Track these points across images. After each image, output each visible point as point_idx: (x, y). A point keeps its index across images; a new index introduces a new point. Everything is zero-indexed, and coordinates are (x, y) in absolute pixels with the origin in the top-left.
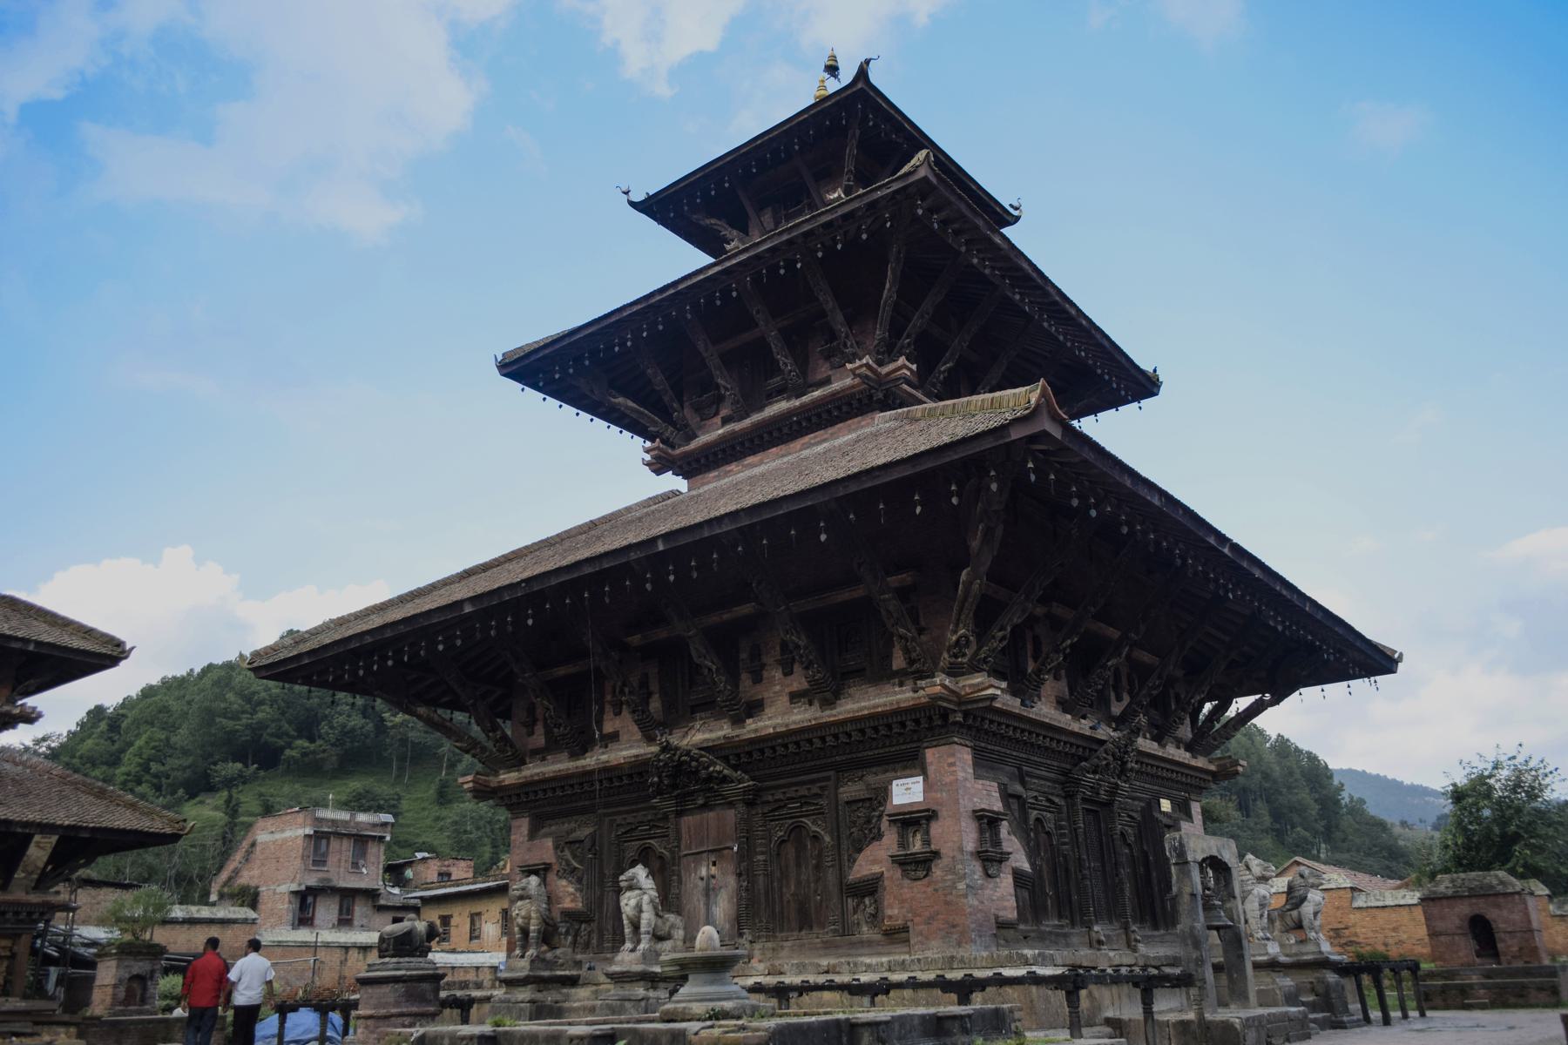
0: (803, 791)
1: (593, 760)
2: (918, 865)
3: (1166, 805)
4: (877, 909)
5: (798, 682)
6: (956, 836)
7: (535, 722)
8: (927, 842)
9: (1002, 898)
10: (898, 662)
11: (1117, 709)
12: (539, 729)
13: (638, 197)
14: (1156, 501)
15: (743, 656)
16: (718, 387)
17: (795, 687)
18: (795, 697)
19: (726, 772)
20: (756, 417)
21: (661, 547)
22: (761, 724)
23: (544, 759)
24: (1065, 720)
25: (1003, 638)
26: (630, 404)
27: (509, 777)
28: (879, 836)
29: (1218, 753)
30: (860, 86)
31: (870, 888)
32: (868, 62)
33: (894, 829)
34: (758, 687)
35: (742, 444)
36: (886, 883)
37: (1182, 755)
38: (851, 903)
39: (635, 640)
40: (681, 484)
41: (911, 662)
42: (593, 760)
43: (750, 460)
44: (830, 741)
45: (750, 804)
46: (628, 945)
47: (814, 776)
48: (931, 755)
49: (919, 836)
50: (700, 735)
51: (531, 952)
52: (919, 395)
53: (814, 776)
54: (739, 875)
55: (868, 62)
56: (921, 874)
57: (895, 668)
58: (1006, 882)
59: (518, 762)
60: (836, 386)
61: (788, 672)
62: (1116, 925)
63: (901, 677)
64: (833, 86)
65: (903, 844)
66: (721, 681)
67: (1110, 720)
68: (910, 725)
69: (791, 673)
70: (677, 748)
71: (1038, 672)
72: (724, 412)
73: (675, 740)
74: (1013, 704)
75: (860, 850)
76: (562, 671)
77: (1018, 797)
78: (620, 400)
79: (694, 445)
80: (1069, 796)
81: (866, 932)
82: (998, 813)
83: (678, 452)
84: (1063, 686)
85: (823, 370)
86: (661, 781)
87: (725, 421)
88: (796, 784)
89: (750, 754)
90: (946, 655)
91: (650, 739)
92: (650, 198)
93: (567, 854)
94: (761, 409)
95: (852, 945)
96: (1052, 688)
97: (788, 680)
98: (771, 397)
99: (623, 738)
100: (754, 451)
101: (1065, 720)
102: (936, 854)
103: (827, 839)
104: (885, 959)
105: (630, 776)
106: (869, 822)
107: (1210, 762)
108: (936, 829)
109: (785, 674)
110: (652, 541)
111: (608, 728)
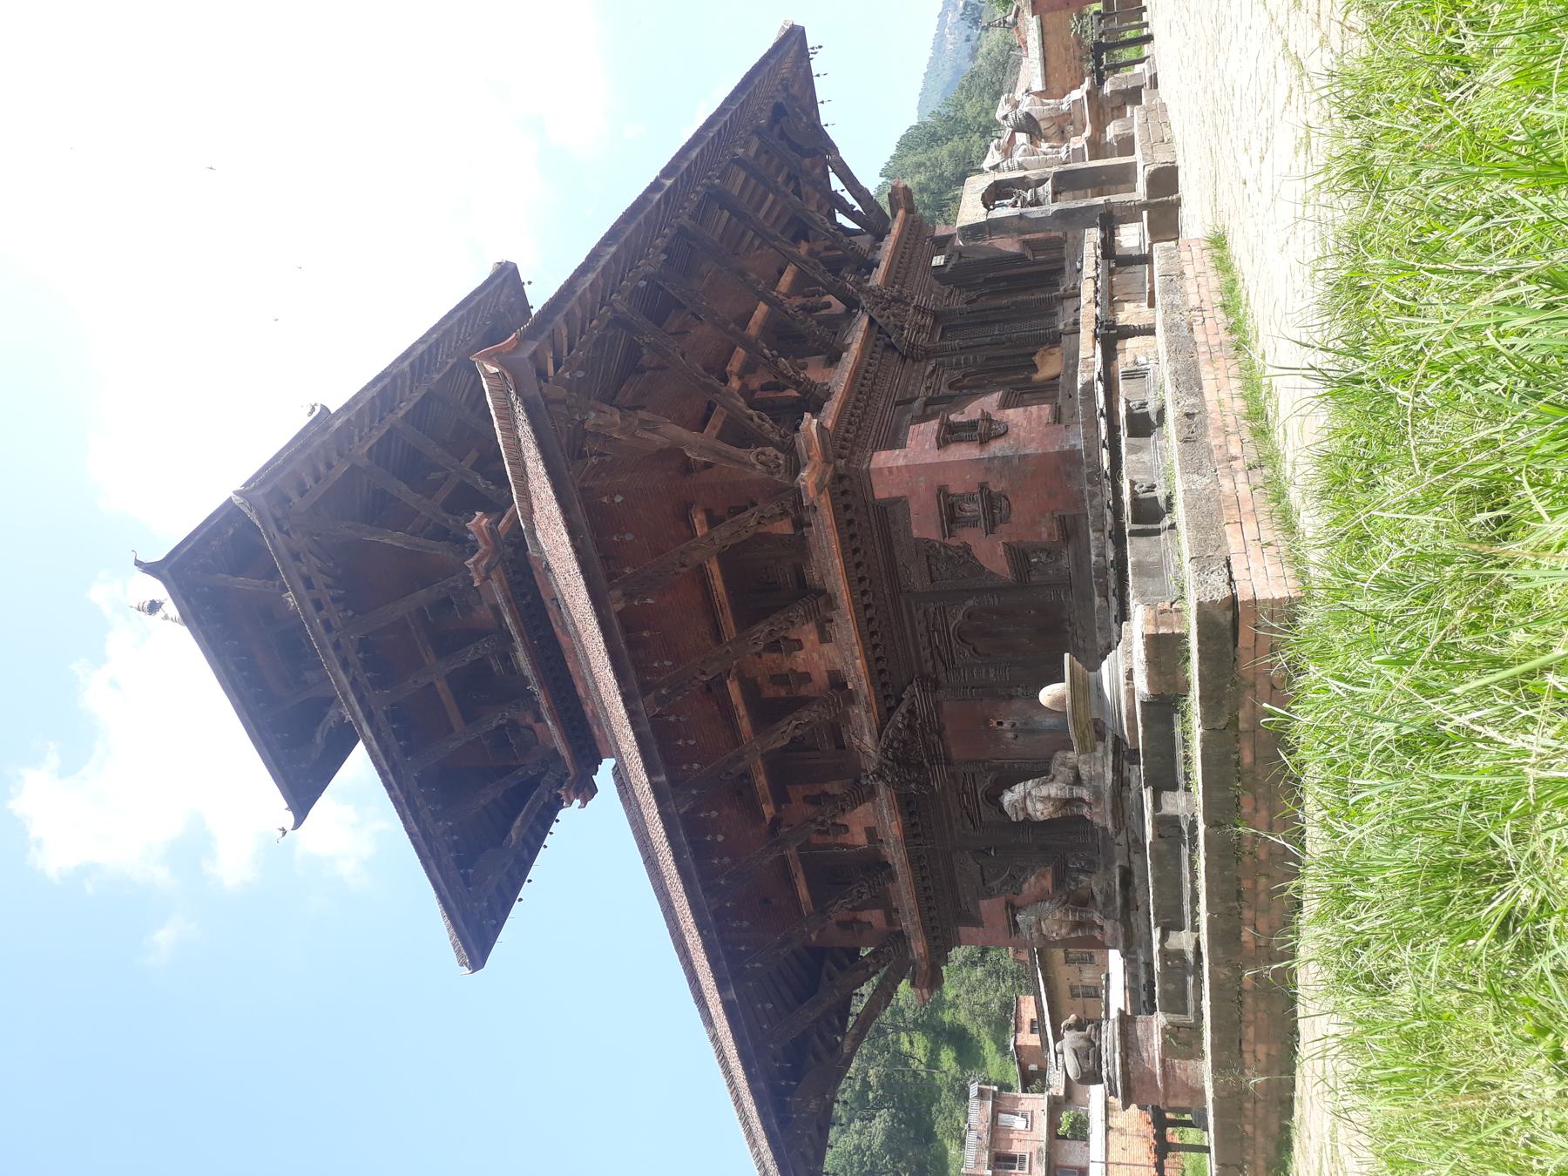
0: (923, 625)
1: (896, 855)
2: (994, 507)
3: (938, 261)
4: (1042, 550)
5: (808, 634)
7: (855, 921)
8: (971, 499)
9: (1029, 421)
10: (784, 527)
11: (838, 307)
12: (865, 916)
13: (289, 818)
14: (613, 249)
15: (783, 693)
16: (500, 728)
19: (903, 710)
20: (534, 687)
21: (663, 778)
23: (897, 910)
24: (850, 358)
25: (760, 417)
26: (518, 823)
27: (918, 947)
28: (967, 548)
29: (888, 211)
30: (165, 572)
31: (1018, 555)
32: (138, 563)
33: (958, 532)
34: (815, 676)
36: (1014, 540)
37: (889, 244)
38: (1035, 578)
39: (768, 810)
40: (607, 765)
41: (784, 513)
42: (896, 855)
43: (581, 691)
45: (937, 685)
46: (1085, 811)
47: (906, 617)
48: (881, 492)
49: (966, 506)
50: (866, 740)
51: (1097, 918)
52: (510, 511)
53: (906, 617)
54: (1011, 697)
55: (138, 563)
56: (1004, 503)
57: (791, 531)
58: (1013, 415)
59: (901, 938)
60: (500, 599)
62: (1059, 309)
63: (799, 524)
64: (170, 608)
66: (806, 716)
67: (849, 315)
70: (880, 763)
71: (798, 384)
72: (529, 720)
73: (872, 767)
74: (831, 408)
75: (982, 567)
76: (803, 892)
77: (926, 404)
78: (513, 834)
79: (564, 751)
80: (928, 354)
81: (1066, 561)
82: (941, 424)
83: (571, 770)
84: (813, 361)
86: (915, 781)
87: (539, 718)
88: (915, 637)
89: (884, 685)
90: (777, 477)
91: (872, 793)
92: (291, 808)
93: (995, 884)
94: (526, 681)
96: (815, 373)
97: (807, 645)
98: (513, 671)
99: (872, 822)
101: (850, 358)
102: (983, 486)
103: (970, 603)
104: (1092, 536)
105: (911, 814)
106: (951, 558)
107: (894, 216)
108: (956, 488)
109: (801, 648)
111: (861, 839)
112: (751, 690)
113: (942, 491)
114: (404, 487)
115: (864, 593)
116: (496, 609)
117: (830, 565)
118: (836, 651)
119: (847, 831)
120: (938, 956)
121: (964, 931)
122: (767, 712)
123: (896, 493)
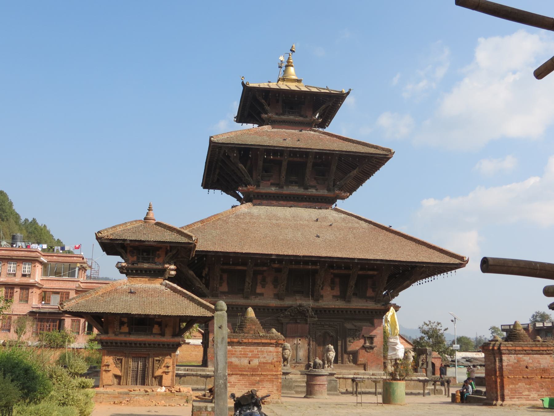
17: (335, 294)
18: (334, 297)
22: (324, 303)
32: (350, 90)
35: (282, 197)
38: (345, 356)
43: (282, 202)
44: (349, 312)
45: (313, 324)
48: (376, 321)
55: (350, 90)
57: (368, 295)
61: (332, 289)
63: (371, 298)
68: (374, 313)
72: (272, 181)
85: (313, 183)
87: (272, 184)
89: (320, 311)
95: (346, 366)
100: (284, 200)
105: (272, 310)
110: (354, 259)
115: (351, 311)
117: (358, 304)
119: (262, 287)
123: (376, 325)
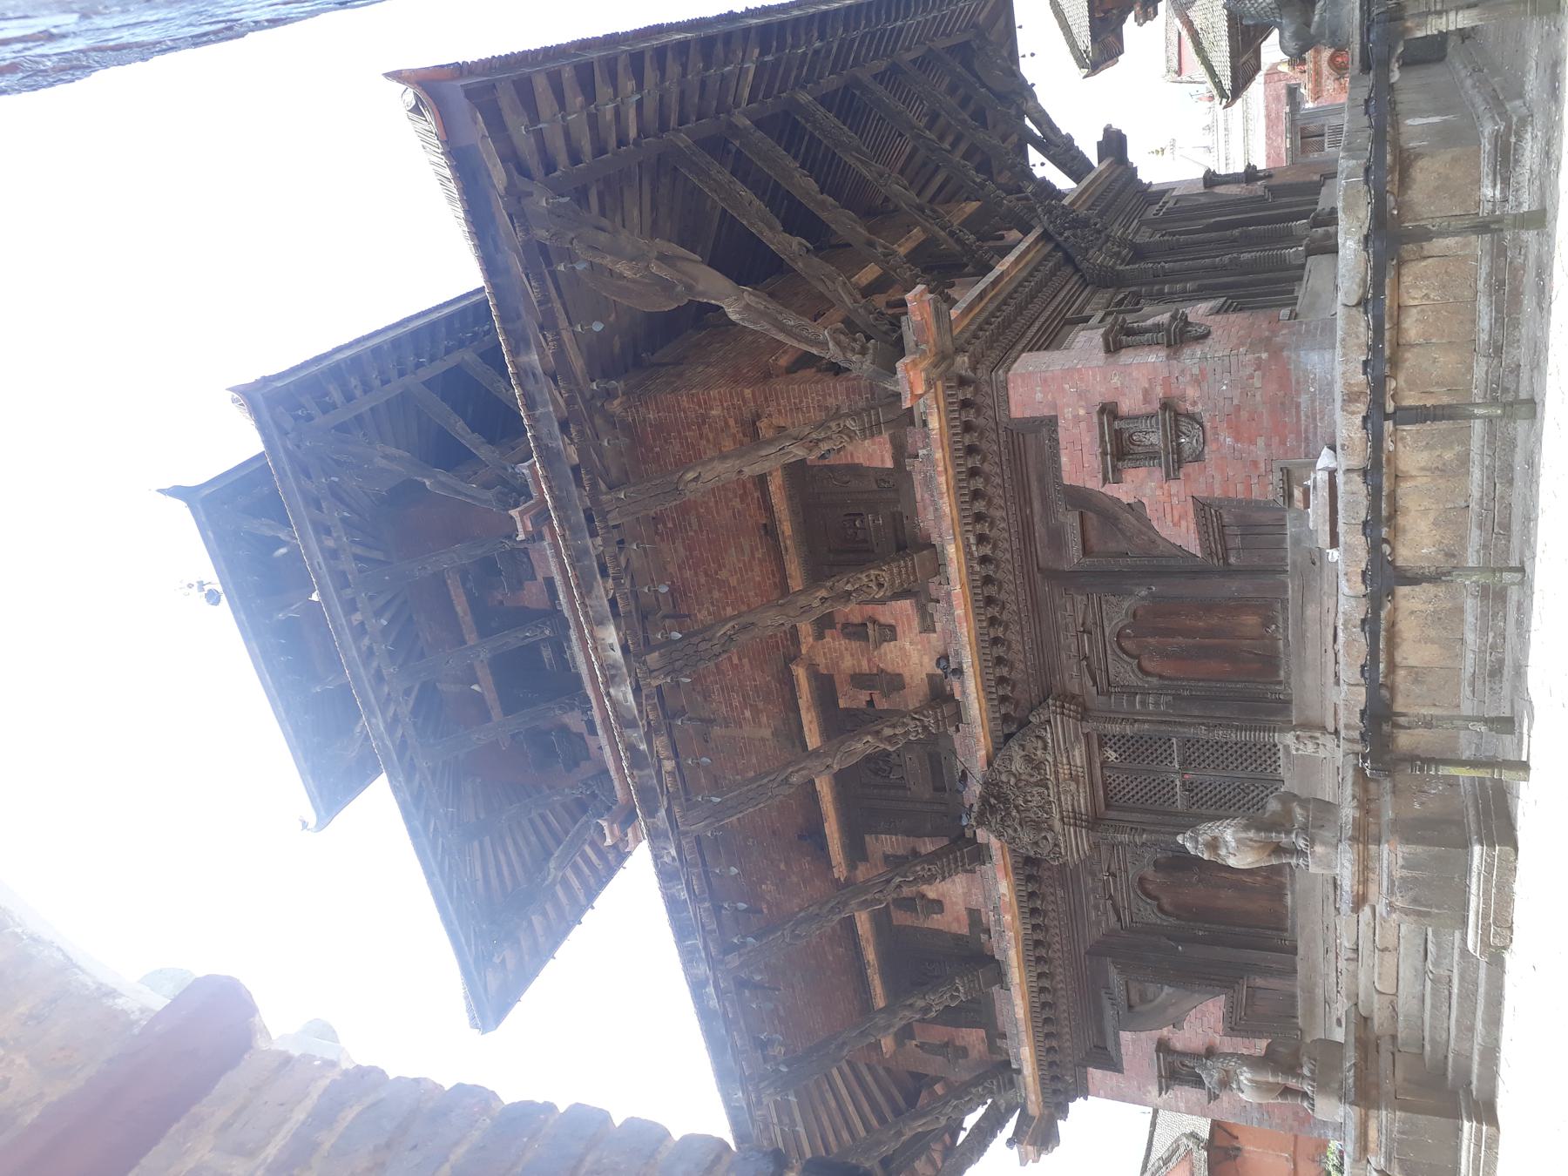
6: (1139, 377)
13: (312, 819)
18: (928, 627)
23: (1004, 1036)
57: (889, 464)
61: (889, 633)
63: (901, 452)
65: (1152, 456)
69: (892, 628)
72: (581, 728)
87: (592, 730)
91: (980, 854)
102: (1166, 406)
112: (825, 687)
113: (1109, 411)
114: (461, 423)
116: (550, 582)
118: (934, 639)
120: (1058, 1108)
121: (1095, 1074)
122: (839, 724)
